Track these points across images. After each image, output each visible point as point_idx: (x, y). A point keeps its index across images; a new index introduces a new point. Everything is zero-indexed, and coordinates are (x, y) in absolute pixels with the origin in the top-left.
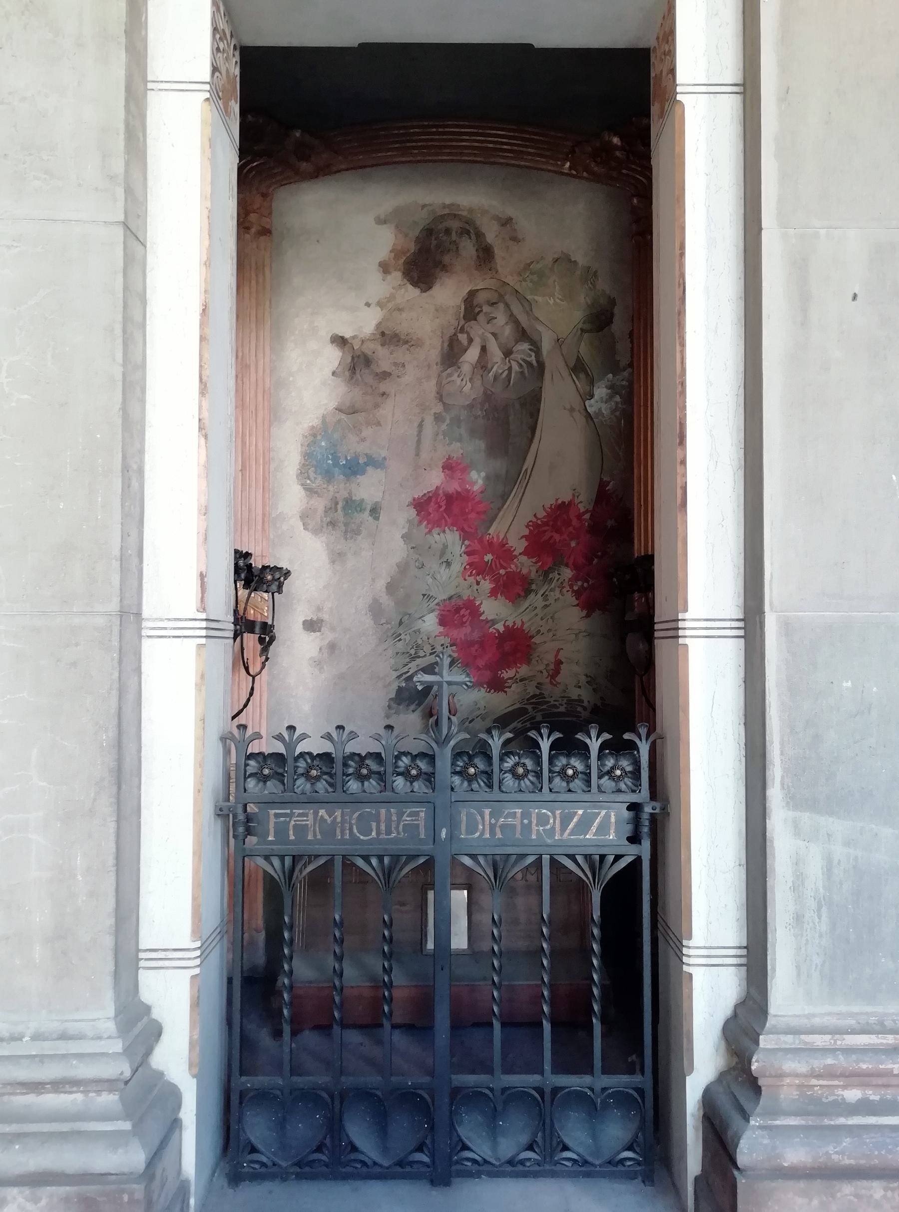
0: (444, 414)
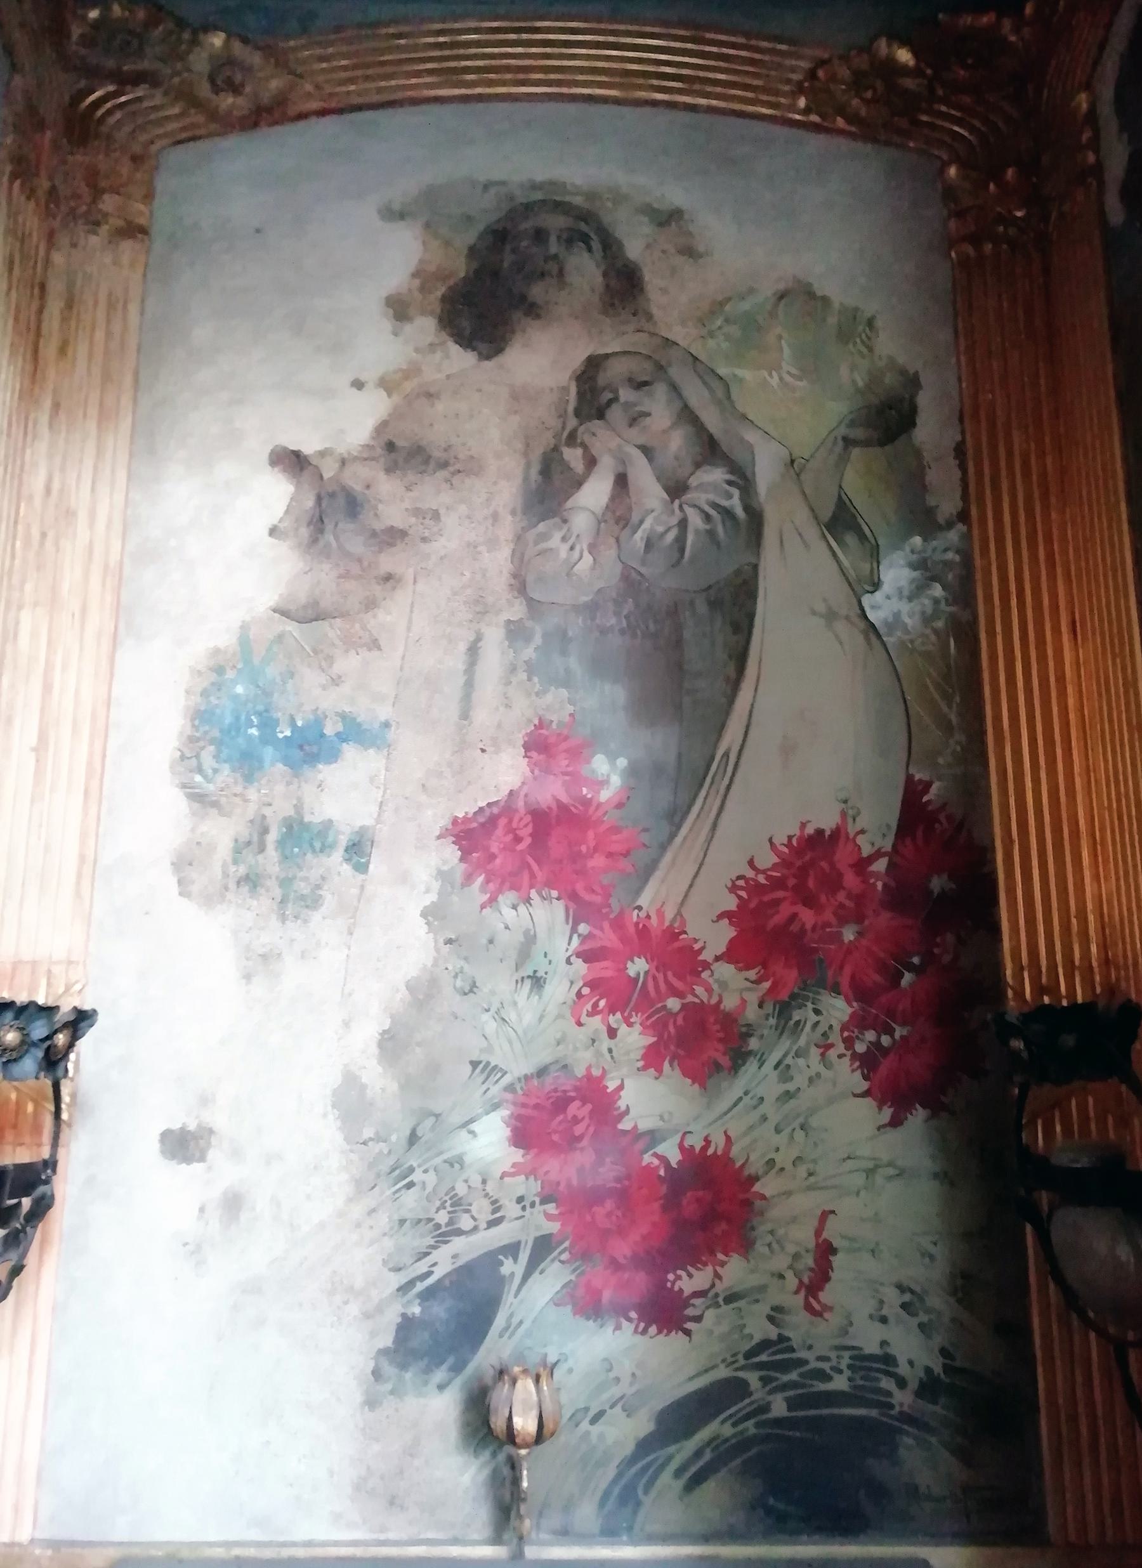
0: (529, 624)
